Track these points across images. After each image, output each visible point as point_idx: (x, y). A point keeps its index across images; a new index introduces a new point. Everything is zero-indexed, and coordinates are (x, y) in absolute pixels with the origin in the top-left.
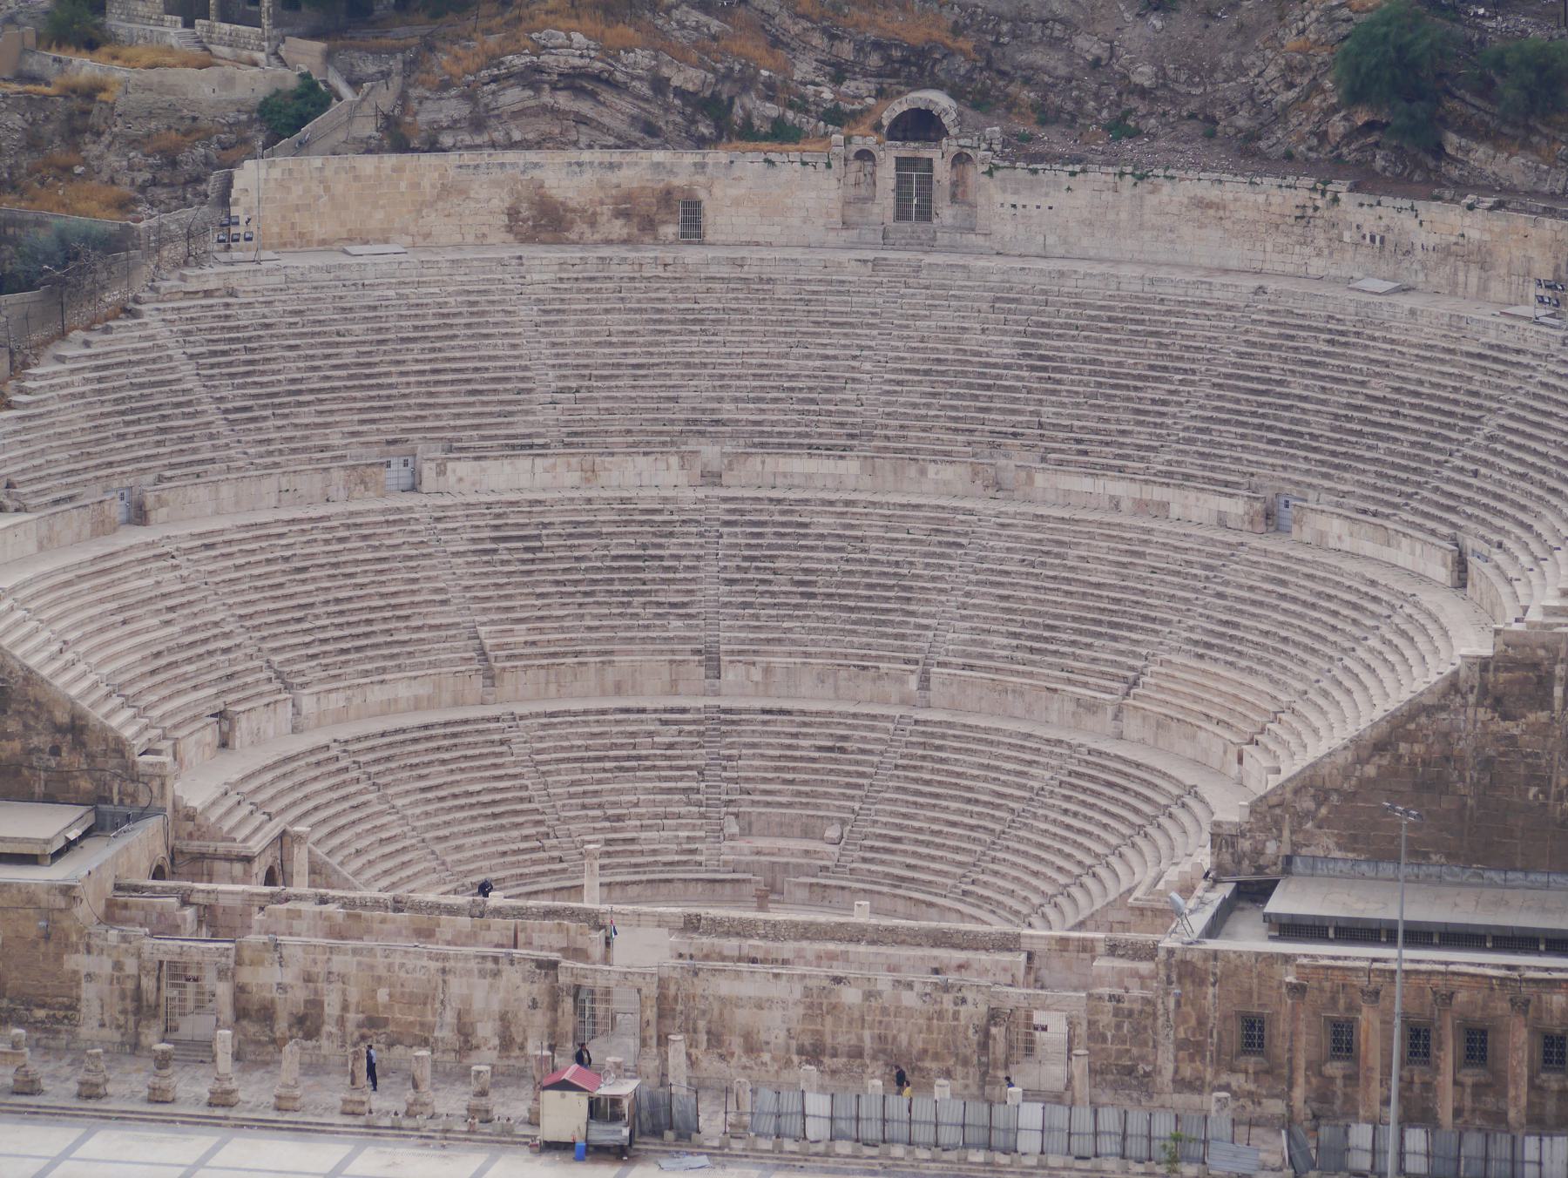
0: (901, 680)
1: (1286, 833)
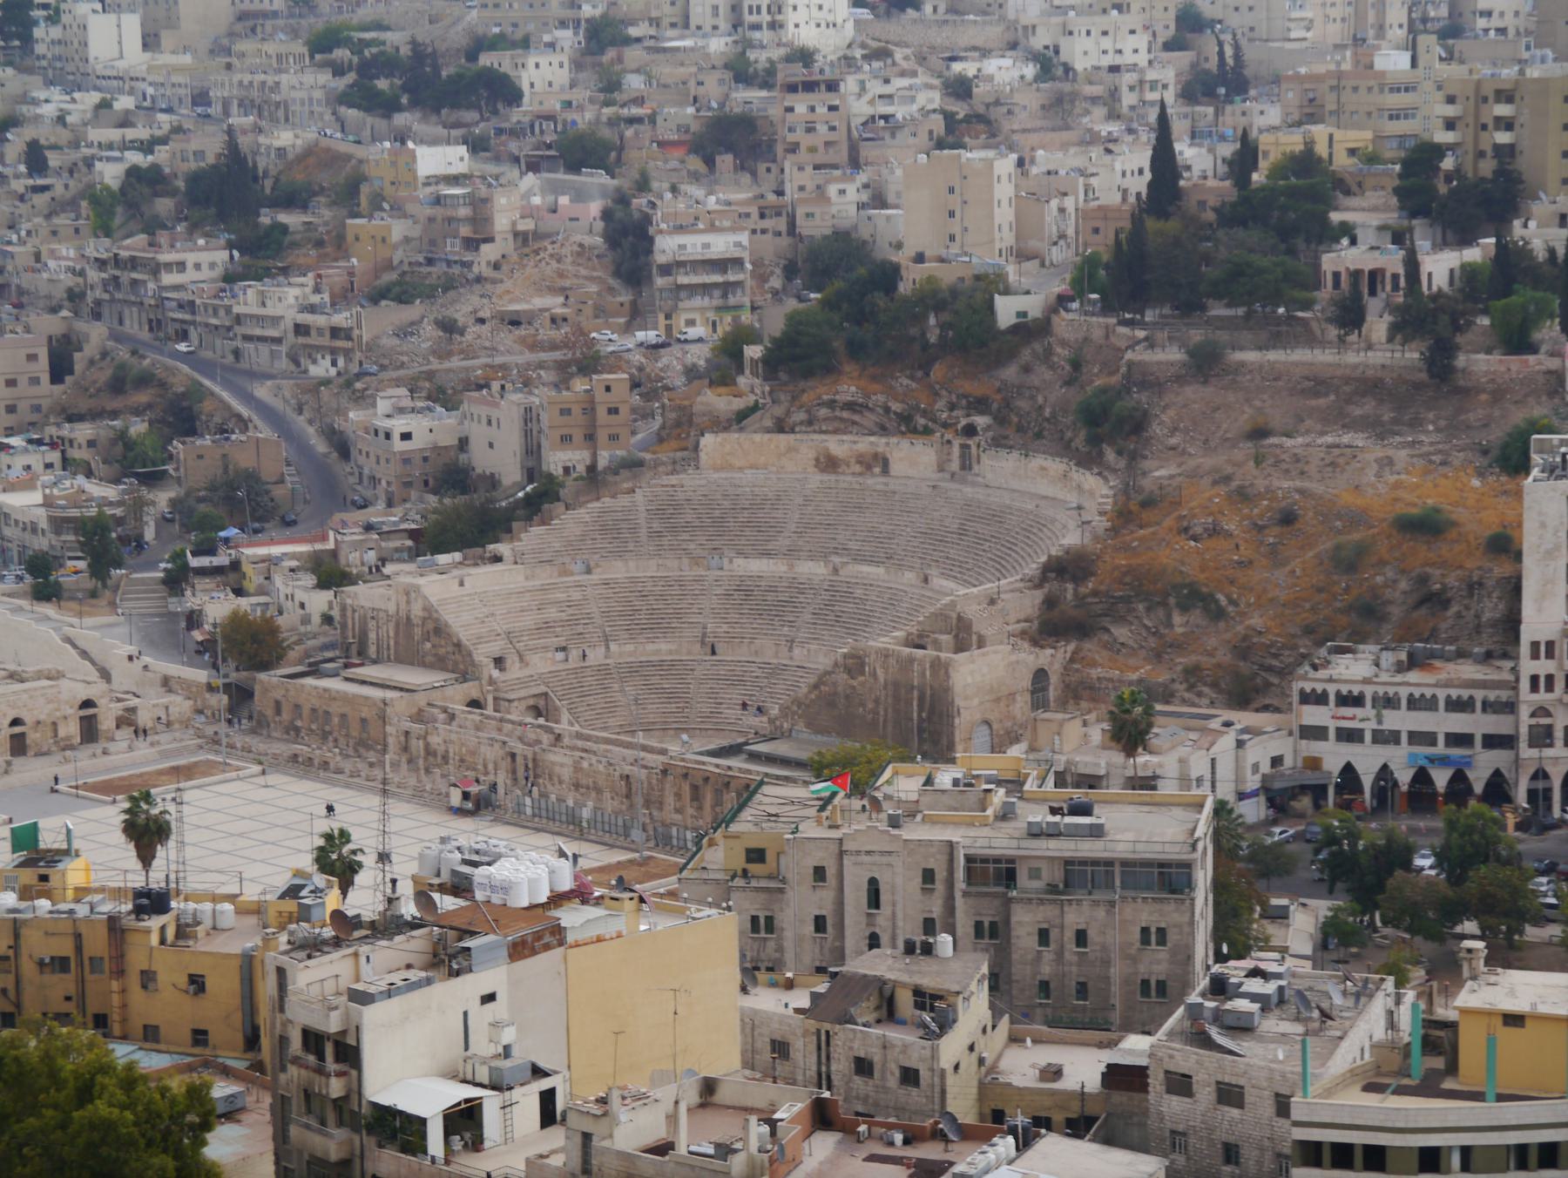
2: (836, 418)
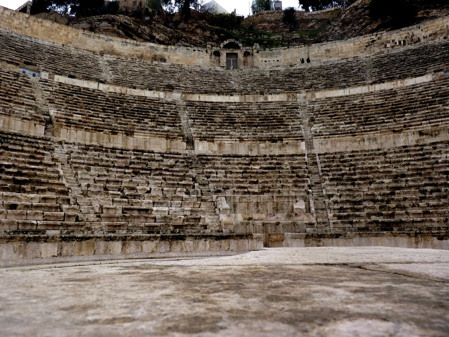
0: (297, 146)
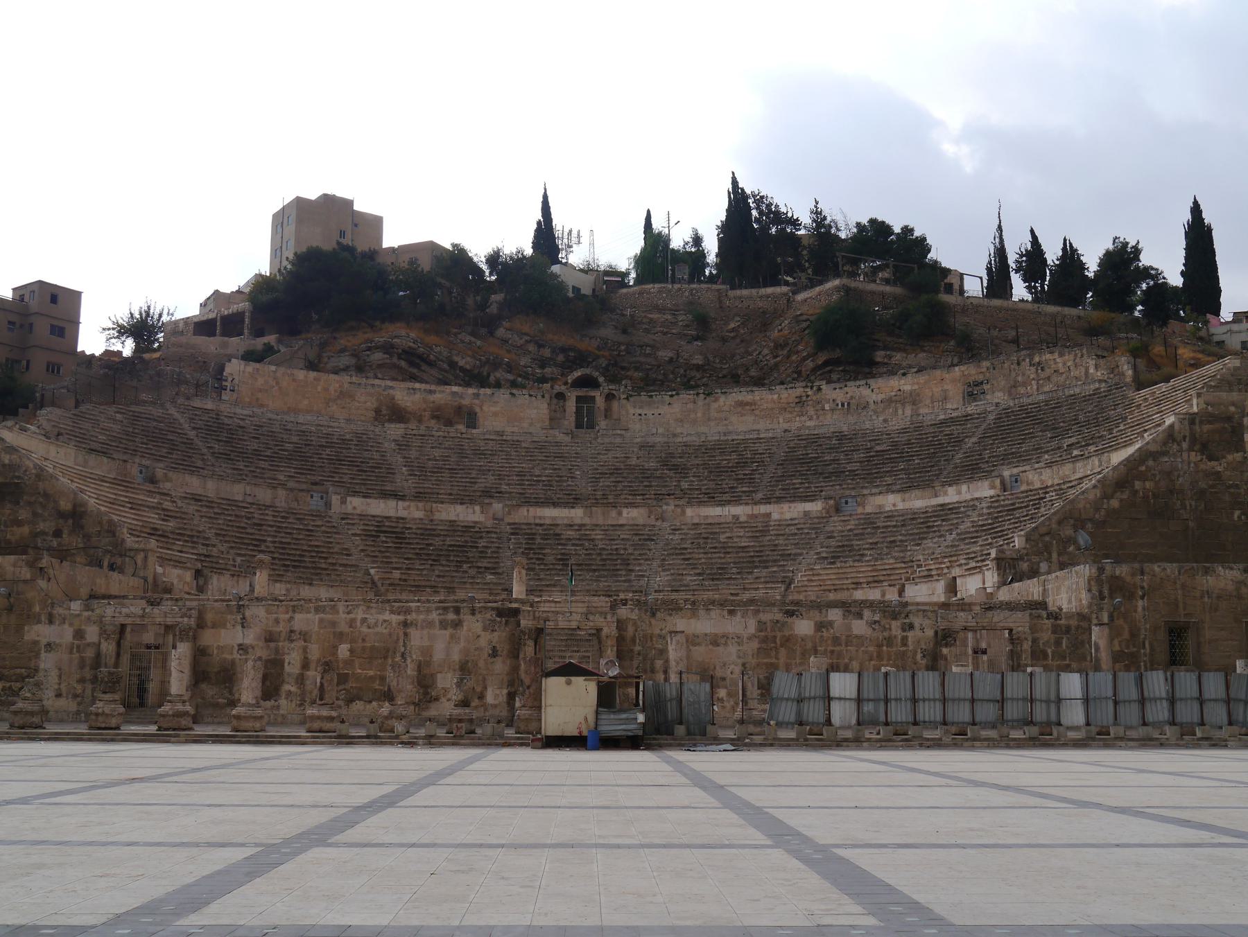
1: (1055, 556)
2: (395, 366)
